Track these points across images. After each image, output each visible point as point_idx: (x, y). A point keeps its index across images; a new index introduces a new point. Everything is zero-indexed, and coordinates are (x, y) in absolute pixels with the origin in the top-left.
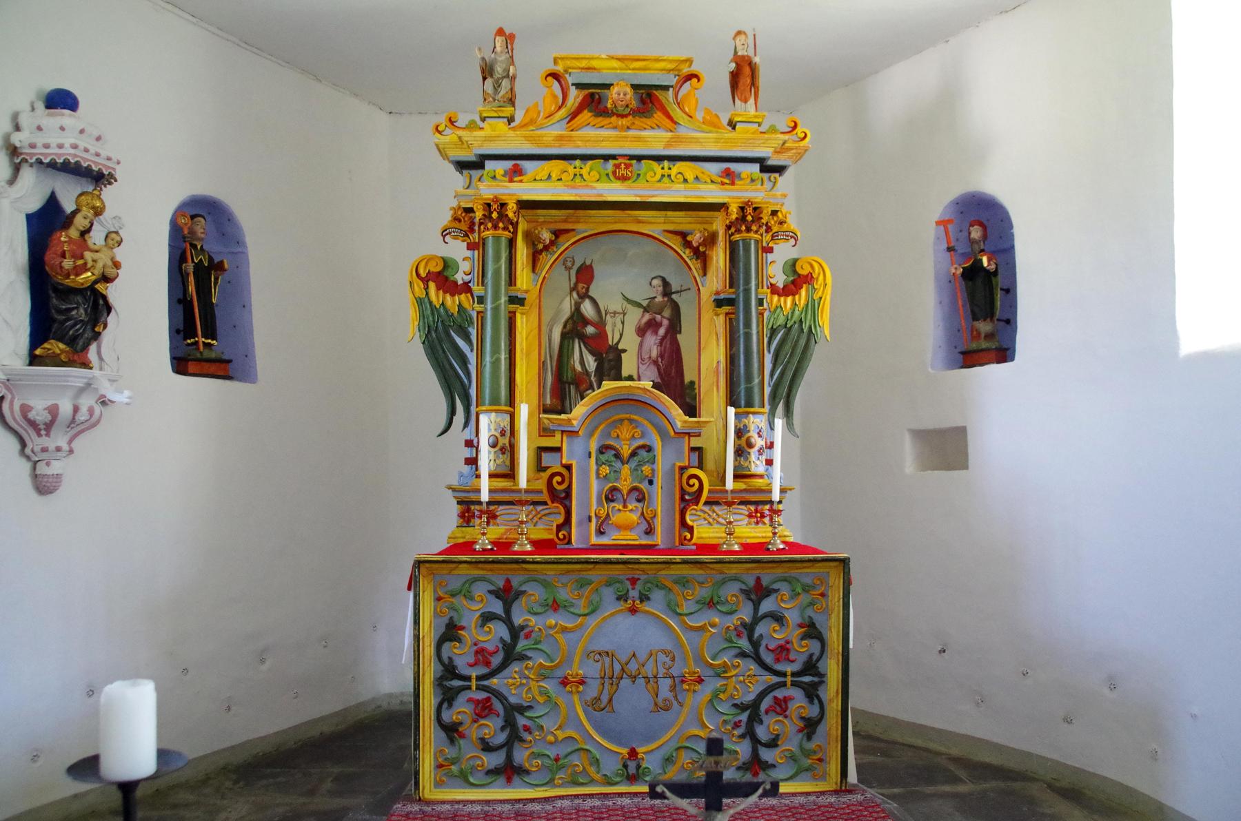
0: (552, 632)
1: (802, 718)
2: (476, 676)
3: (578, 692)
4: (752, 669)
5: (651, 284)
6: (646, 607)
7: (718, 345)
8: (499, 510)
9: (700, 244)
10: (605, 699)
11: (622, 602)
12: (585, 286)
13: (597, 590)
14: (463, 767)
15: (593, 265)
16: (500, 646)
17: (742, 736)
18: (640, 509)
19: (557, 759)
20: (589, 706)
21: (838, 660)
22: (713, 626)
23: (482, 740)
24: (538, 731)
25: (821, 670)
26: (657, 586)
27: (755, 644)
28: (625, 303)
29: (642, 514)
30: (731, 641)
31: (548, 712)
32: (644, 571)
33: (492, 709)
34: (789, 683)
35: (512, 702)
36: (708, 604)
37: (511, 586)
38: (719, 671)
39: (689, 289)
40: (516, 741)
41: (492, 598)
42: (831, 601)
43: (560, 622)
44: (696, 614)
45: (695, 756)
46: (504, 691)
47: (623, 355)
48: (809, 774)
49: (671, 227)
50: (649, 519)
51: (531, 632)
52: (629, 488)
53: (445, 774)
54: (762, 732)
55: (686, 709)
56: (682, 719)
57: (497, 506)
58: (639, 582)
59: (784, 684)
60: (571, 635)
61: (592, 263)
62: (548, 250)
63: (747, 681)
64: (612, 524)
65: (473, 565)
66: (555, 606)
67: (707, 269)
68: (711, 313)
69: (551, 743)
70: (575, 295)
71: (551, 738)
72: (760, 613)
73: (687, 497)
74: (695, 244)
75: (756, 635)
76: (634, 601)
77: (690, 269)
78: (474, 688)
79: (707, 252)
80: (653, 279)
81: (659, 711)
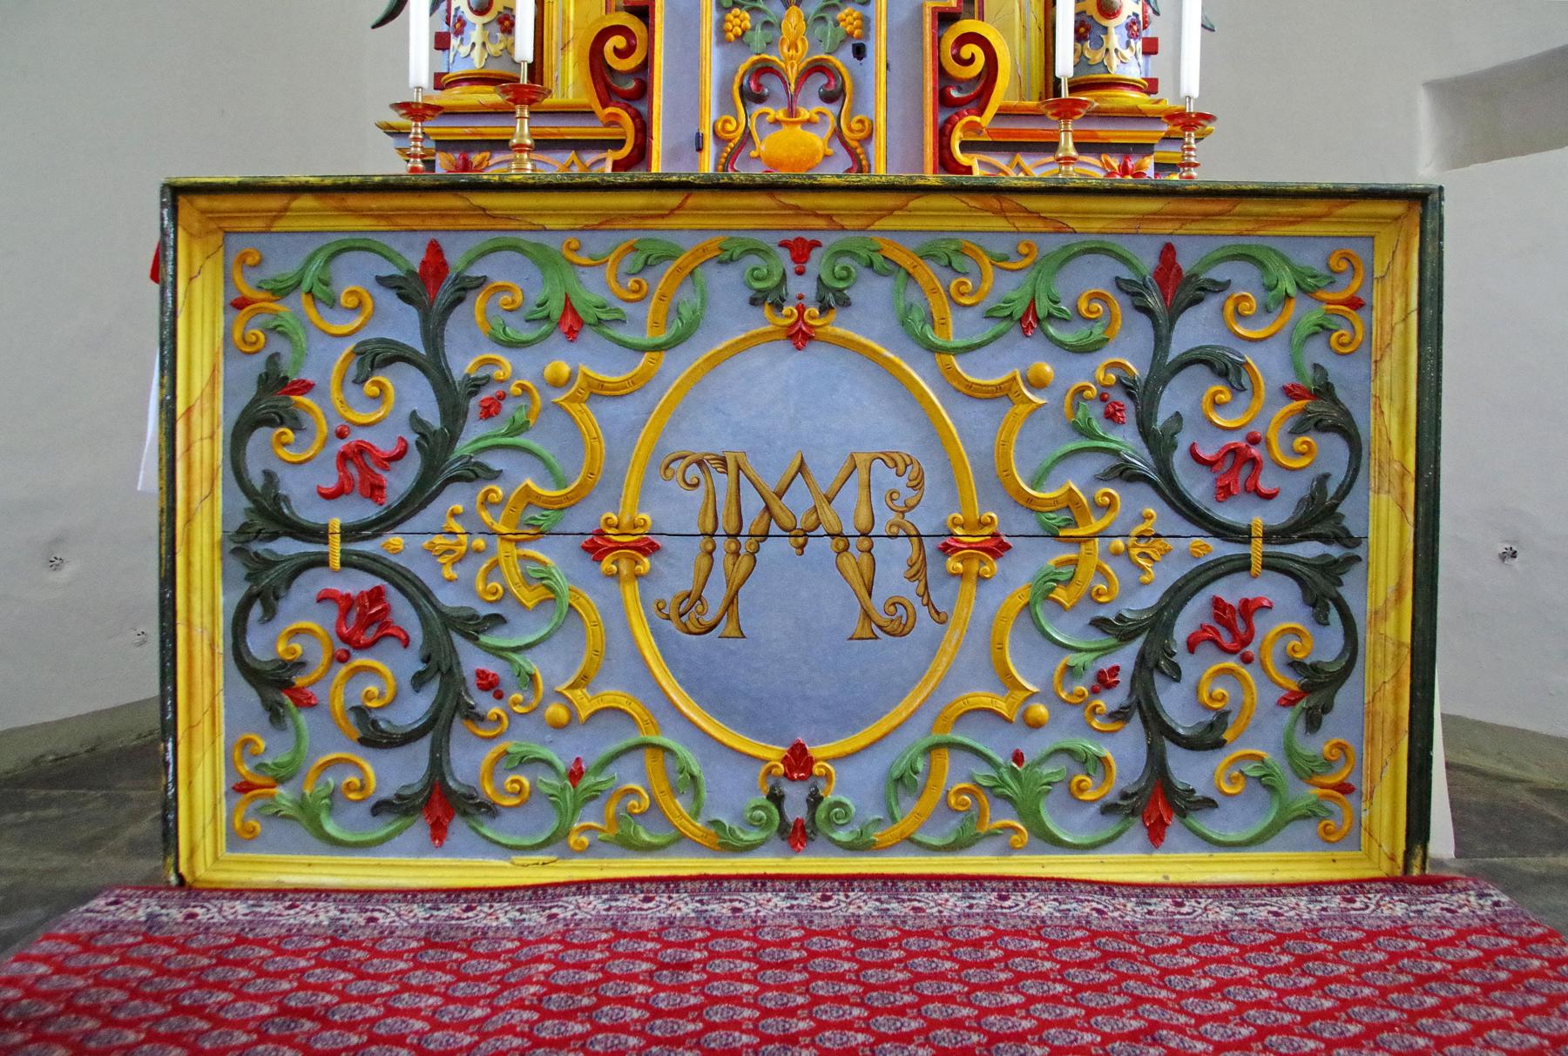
0: (559, 398)
1: (1295, 665)
2: (341, 526)
3: (638, 576)
4: (1151, 517)
6: (835, 326)
8: (491, 162)
10: (715, 597)
11: (767, 311)
13: (692, 273)
14: (308, 792)
16: (412, 438)
17: (1121, 715)
18: (831, 119)
19: (575, 775)
20: (668, 618)
21: (1403, 495)
22: (1037, 385)
23: (361, 712)
24: (520, 690)
25: (1352, 525)
26: (870, 265)
27: (1159, 443)
29: (838, 132)
30: (1089, 433)
31: (549, 636)
32: (829, 217)
33: (387, 625)
34: (1256, 562)
35: (447, 604)
36: (1021, 320)
37: (444, 264)
38: (1056, 519)
40: (457, 719)
41: (389, 299)
42: (1382, 321)
43: (584, 368)
44: (984, 352)
45: (982, 772)
46: (421, 570)
48: (1308, 830)
50: (853, 144)
51: (502, 396)
52: (804, 64)
53: (257, 810)
54: (1175, 704)
55: (953, 636)
56: (941, 664)
57: (487, 154)
58: (815, 254)
59: (1241, 565)
60: (610, 408)
63: (1134, 552)
64: (759, 157)
65: (331, 202)
66: (572, 324)
69: (558, 727)
71: (557, 711)
72: (1176, 350)
73: (955, 94)
75: (1162, 417)
76: (801, 309)
78: (335, 561)
81: (877, 638)
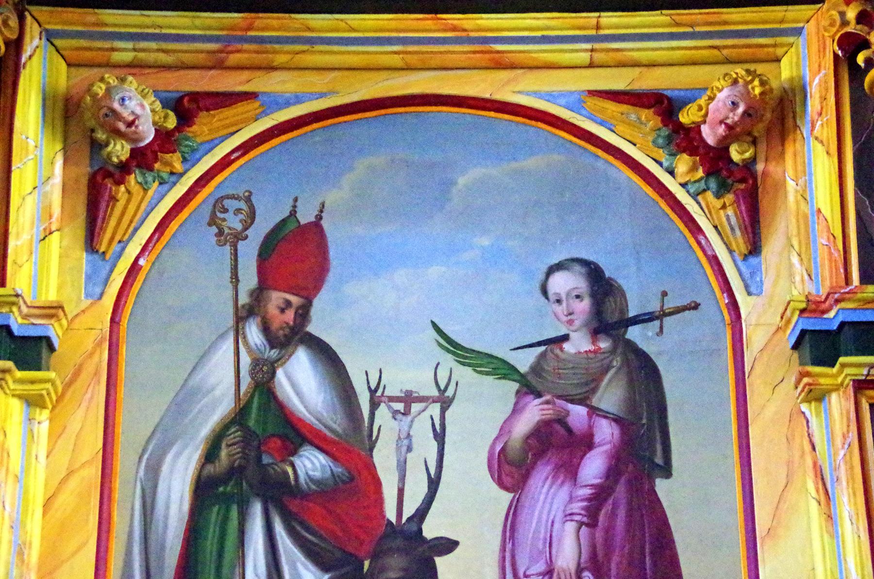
5: (544, 291)
7: (830, 518)
9: (733, 133)
12: (295, 300)
15: (325, 224)
28: (448, 361)
39: (695, 306)
47: (439, 561)
49: (619, 80)
61: (319, 218)
62: (151, 169)
67: (764, 232)
68: (788, 392)
70: (254, 334)
74: (710, 135)
77: (696, 229)
79: (760, 167)
80: (552, 270)
